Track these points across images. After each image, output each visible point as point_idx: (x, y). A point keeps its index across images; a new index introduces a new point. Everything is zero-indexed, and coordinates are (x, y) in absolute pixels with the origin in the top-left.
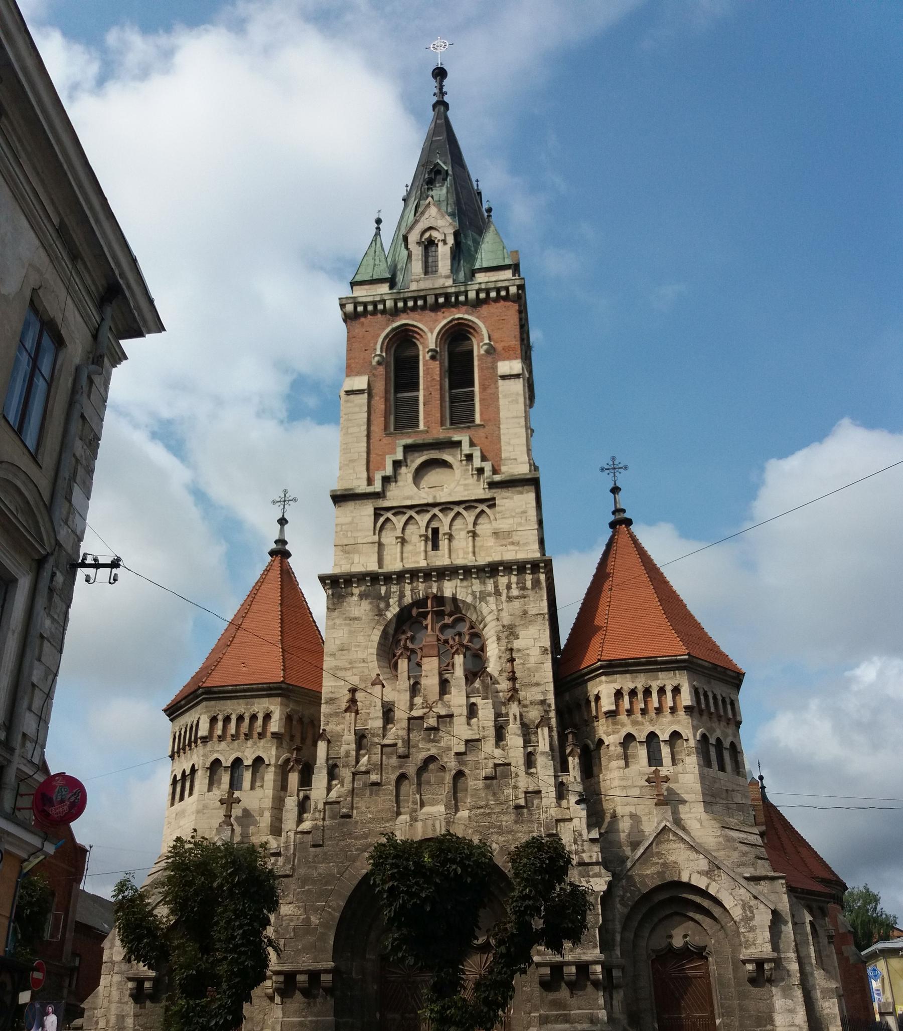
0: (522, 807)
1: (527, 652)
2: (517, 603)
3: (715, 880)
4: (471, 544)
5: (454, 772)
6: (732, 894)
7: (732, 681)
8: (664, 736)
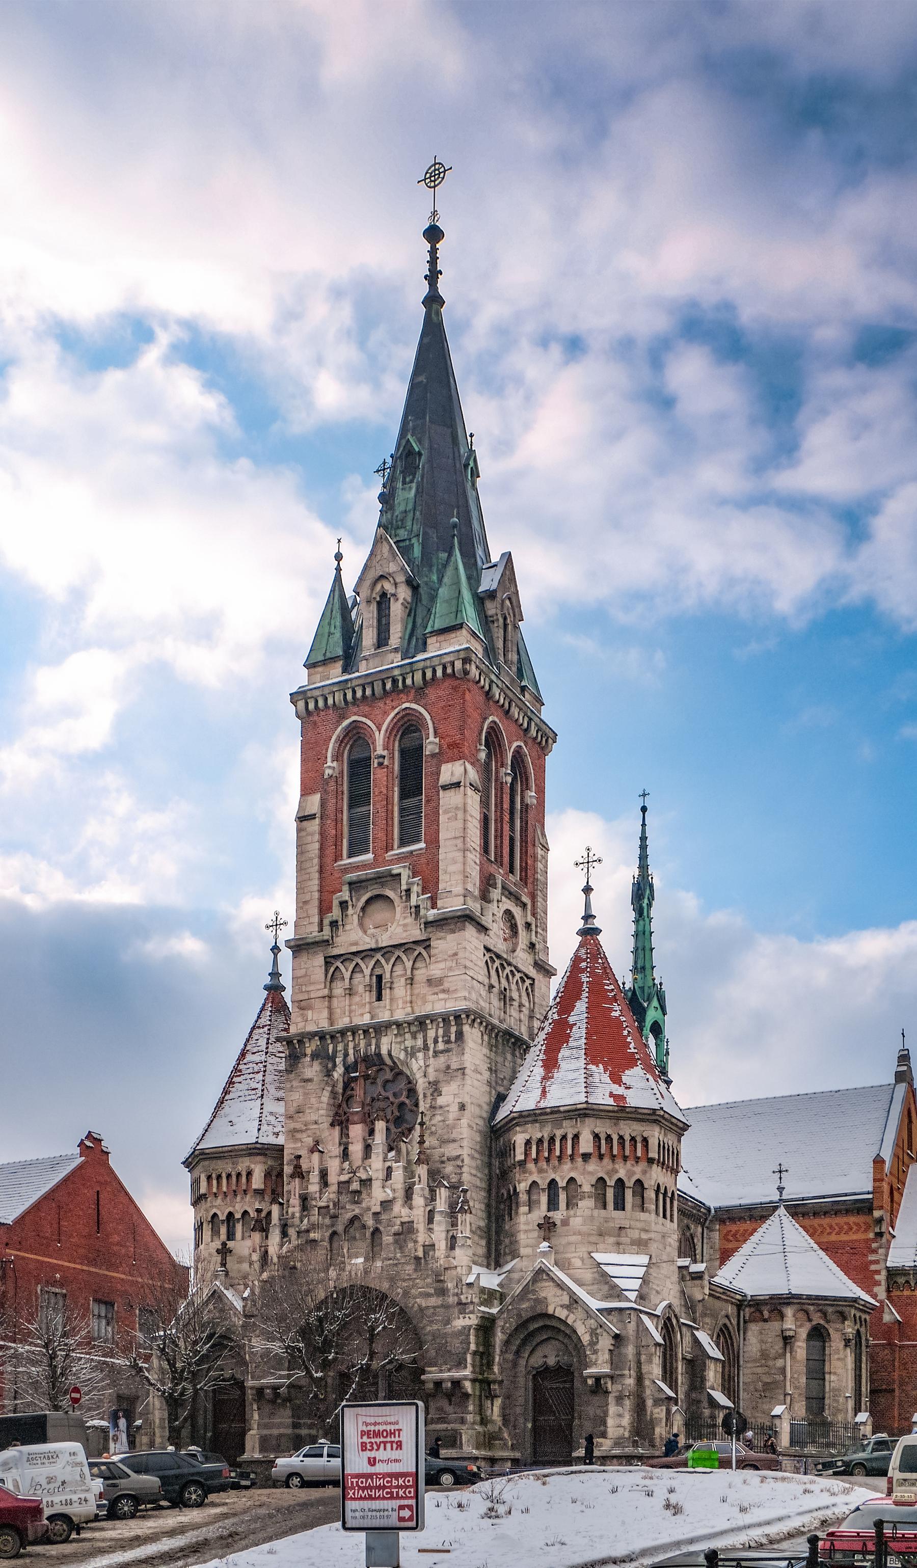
0: (421, 1258)
1: (447, 1109)
2: (442, 1059)
3: (573, 1313)
4: (408, 993)
5: (372, 1229)
6: (584, 1323)
7: (648, 1117)
8: (562, 1183)
